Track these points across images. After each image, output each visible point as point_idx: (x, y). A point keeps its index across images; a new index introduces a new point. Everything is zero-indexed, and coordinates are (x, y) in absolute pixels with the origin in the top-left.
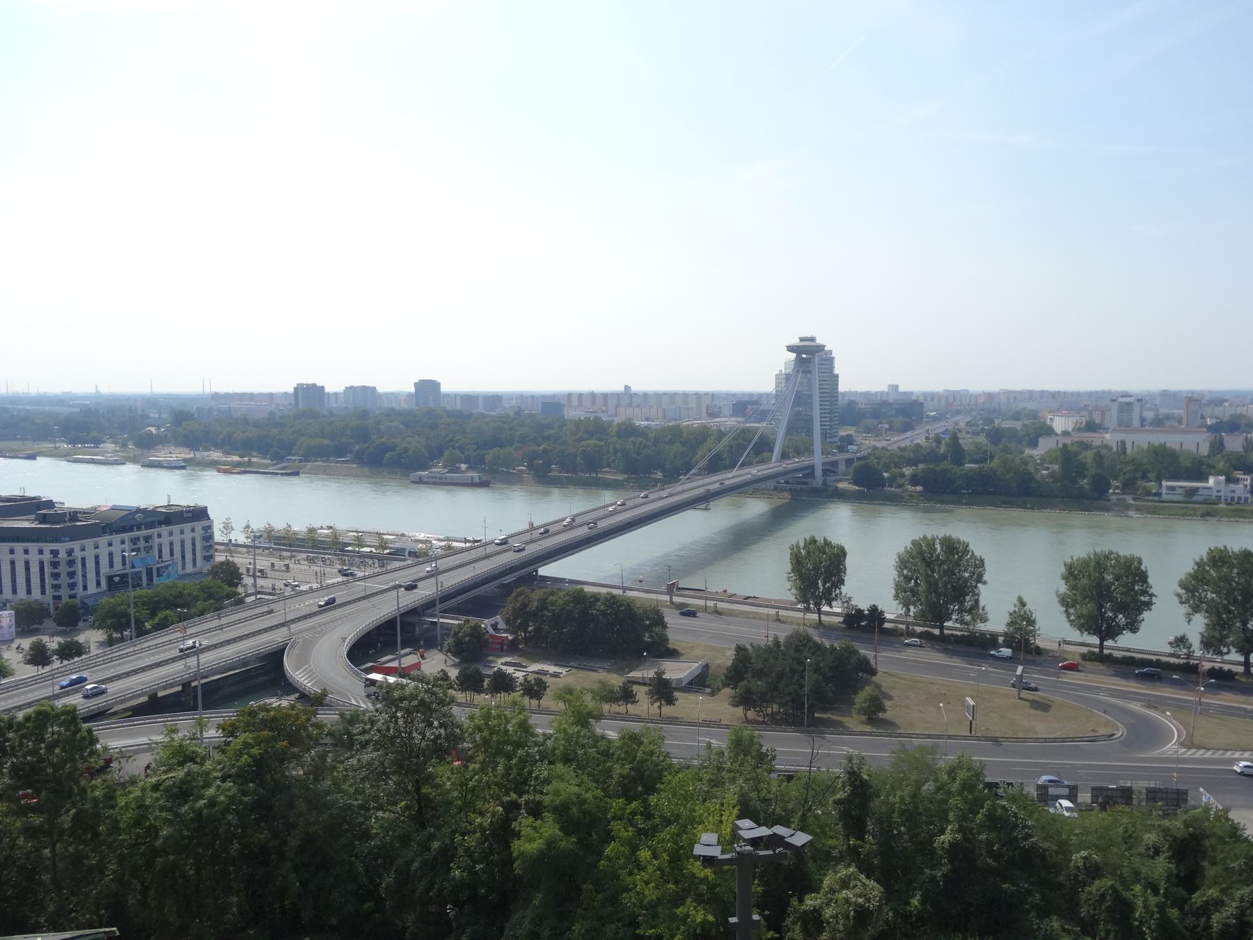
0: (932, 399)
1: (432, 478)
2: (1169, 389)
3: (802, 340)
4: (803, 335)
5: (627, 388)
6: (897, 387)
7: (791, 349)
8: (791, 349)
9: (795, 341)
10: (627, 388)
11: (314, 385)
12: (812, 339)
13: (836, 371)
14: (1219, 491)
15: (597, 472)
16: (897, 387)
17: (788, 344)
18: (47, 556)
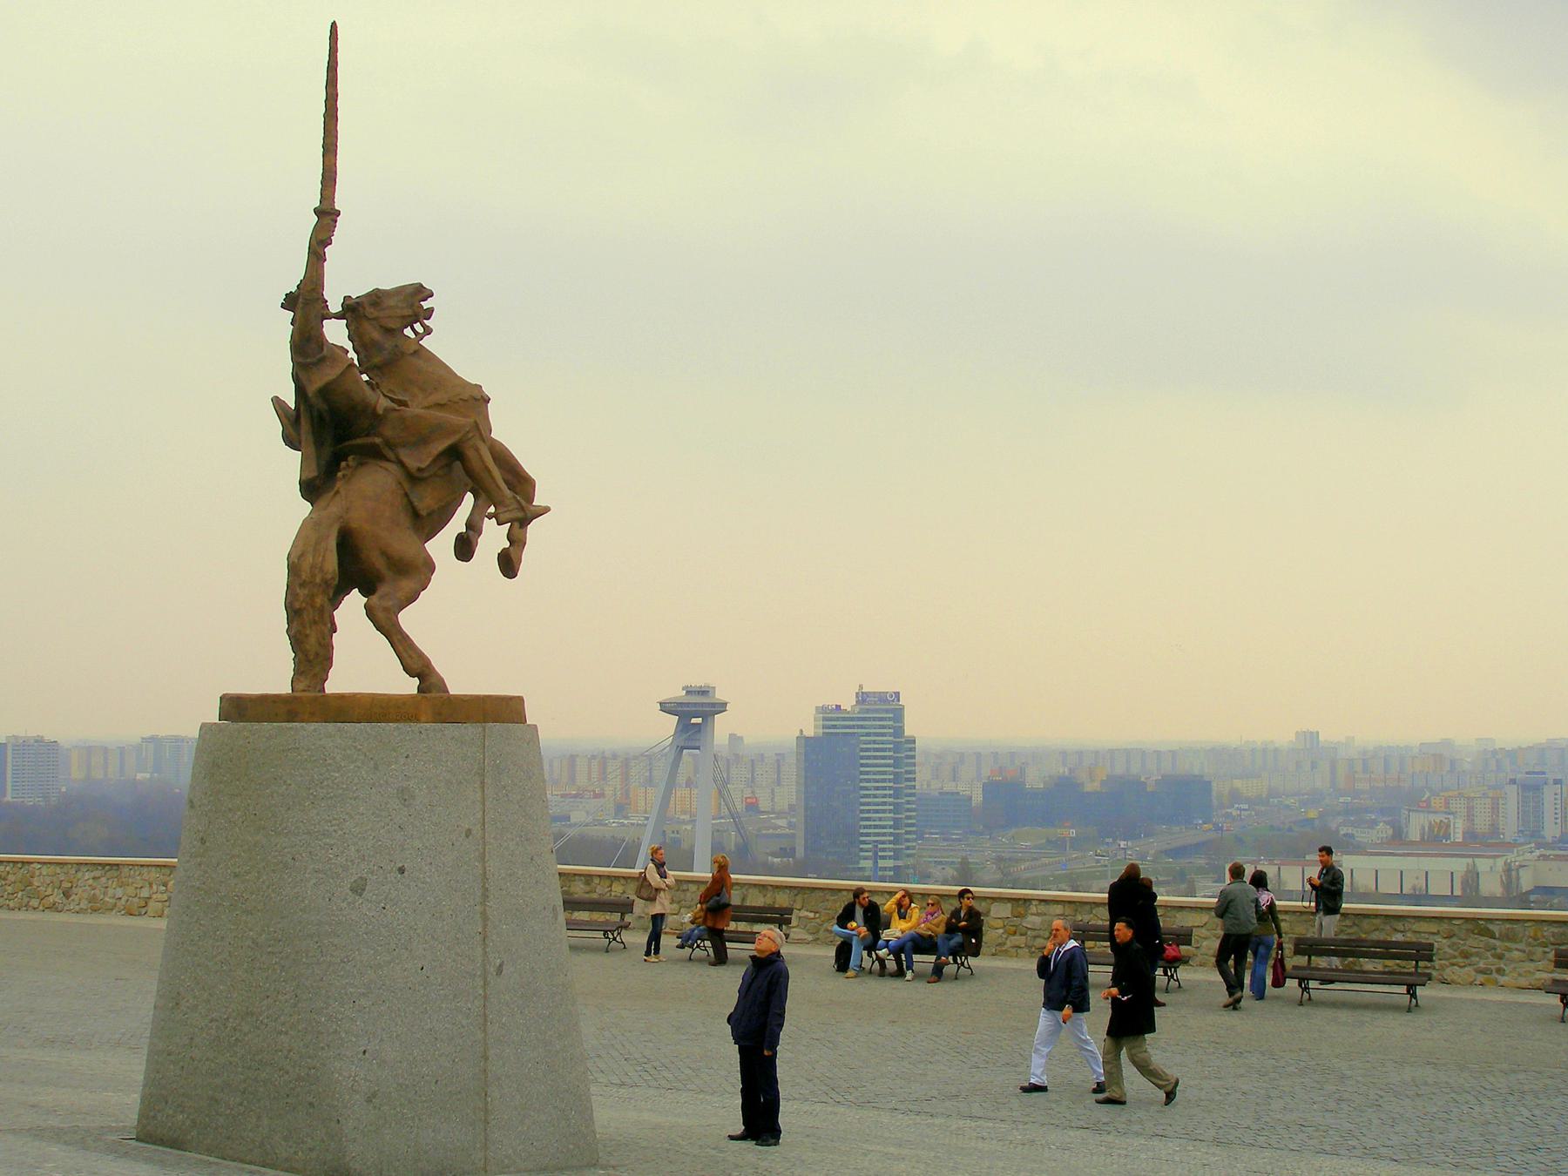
0: (1314, 766)
4: (697, 682)
7: (666, 707)
8: (666, 707)
12: (703, 692)
17: (660, 700)
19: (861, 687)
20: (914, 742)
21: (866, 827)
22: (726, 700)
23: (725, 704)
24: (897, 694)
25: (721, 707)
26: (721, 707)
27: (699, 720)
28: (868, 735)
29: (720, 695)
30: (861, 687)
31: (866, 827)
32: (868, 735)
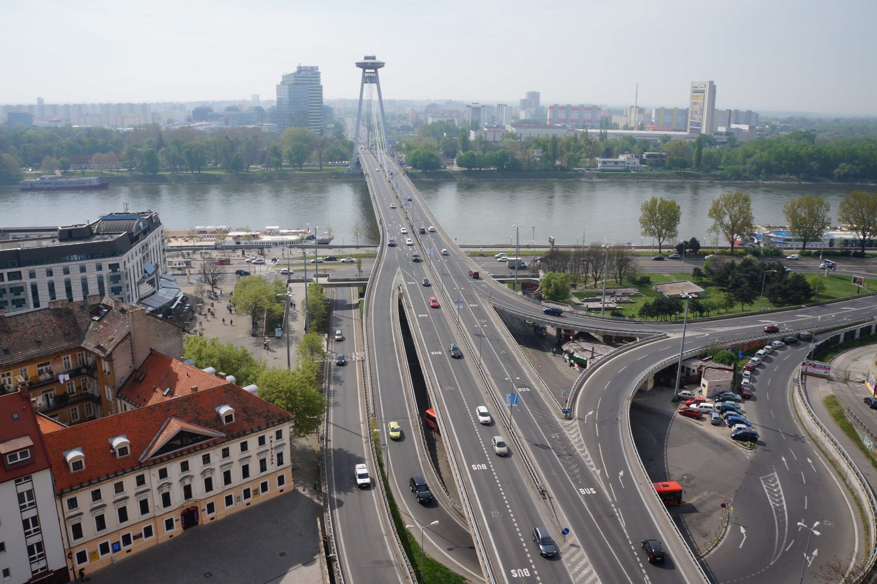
1: (46, 184)
2: (453, 99)
3: (366, 58)
5: (40, 100)
6: (258, 96)
7: (359, 65)
8: (359, 65)
9: (362, 60)
10: (40, 100)
11: (534, 92)
12: (374, 58)
13: (322, 83)
14: (628, 164)
15: (199, 170)
16: (258, 96)
18: (106, 271)
19: (300, 64)
20: (322, 87)
21: (311, 122)
22: (383, 61)
23: (384, 63)
24: (317, 68)
25: (381, 65)
26: (381, 65)
27: (373, 71)
28: (311, 84)
29: (379, 59)
30: (300, 64)
31: (311, 122)
32: (311, 84)
